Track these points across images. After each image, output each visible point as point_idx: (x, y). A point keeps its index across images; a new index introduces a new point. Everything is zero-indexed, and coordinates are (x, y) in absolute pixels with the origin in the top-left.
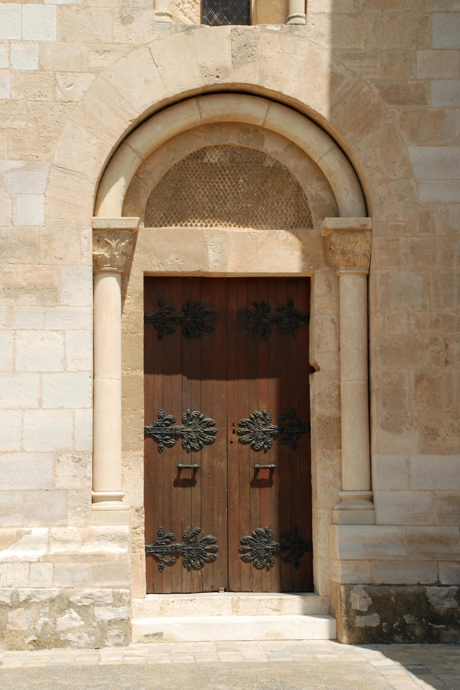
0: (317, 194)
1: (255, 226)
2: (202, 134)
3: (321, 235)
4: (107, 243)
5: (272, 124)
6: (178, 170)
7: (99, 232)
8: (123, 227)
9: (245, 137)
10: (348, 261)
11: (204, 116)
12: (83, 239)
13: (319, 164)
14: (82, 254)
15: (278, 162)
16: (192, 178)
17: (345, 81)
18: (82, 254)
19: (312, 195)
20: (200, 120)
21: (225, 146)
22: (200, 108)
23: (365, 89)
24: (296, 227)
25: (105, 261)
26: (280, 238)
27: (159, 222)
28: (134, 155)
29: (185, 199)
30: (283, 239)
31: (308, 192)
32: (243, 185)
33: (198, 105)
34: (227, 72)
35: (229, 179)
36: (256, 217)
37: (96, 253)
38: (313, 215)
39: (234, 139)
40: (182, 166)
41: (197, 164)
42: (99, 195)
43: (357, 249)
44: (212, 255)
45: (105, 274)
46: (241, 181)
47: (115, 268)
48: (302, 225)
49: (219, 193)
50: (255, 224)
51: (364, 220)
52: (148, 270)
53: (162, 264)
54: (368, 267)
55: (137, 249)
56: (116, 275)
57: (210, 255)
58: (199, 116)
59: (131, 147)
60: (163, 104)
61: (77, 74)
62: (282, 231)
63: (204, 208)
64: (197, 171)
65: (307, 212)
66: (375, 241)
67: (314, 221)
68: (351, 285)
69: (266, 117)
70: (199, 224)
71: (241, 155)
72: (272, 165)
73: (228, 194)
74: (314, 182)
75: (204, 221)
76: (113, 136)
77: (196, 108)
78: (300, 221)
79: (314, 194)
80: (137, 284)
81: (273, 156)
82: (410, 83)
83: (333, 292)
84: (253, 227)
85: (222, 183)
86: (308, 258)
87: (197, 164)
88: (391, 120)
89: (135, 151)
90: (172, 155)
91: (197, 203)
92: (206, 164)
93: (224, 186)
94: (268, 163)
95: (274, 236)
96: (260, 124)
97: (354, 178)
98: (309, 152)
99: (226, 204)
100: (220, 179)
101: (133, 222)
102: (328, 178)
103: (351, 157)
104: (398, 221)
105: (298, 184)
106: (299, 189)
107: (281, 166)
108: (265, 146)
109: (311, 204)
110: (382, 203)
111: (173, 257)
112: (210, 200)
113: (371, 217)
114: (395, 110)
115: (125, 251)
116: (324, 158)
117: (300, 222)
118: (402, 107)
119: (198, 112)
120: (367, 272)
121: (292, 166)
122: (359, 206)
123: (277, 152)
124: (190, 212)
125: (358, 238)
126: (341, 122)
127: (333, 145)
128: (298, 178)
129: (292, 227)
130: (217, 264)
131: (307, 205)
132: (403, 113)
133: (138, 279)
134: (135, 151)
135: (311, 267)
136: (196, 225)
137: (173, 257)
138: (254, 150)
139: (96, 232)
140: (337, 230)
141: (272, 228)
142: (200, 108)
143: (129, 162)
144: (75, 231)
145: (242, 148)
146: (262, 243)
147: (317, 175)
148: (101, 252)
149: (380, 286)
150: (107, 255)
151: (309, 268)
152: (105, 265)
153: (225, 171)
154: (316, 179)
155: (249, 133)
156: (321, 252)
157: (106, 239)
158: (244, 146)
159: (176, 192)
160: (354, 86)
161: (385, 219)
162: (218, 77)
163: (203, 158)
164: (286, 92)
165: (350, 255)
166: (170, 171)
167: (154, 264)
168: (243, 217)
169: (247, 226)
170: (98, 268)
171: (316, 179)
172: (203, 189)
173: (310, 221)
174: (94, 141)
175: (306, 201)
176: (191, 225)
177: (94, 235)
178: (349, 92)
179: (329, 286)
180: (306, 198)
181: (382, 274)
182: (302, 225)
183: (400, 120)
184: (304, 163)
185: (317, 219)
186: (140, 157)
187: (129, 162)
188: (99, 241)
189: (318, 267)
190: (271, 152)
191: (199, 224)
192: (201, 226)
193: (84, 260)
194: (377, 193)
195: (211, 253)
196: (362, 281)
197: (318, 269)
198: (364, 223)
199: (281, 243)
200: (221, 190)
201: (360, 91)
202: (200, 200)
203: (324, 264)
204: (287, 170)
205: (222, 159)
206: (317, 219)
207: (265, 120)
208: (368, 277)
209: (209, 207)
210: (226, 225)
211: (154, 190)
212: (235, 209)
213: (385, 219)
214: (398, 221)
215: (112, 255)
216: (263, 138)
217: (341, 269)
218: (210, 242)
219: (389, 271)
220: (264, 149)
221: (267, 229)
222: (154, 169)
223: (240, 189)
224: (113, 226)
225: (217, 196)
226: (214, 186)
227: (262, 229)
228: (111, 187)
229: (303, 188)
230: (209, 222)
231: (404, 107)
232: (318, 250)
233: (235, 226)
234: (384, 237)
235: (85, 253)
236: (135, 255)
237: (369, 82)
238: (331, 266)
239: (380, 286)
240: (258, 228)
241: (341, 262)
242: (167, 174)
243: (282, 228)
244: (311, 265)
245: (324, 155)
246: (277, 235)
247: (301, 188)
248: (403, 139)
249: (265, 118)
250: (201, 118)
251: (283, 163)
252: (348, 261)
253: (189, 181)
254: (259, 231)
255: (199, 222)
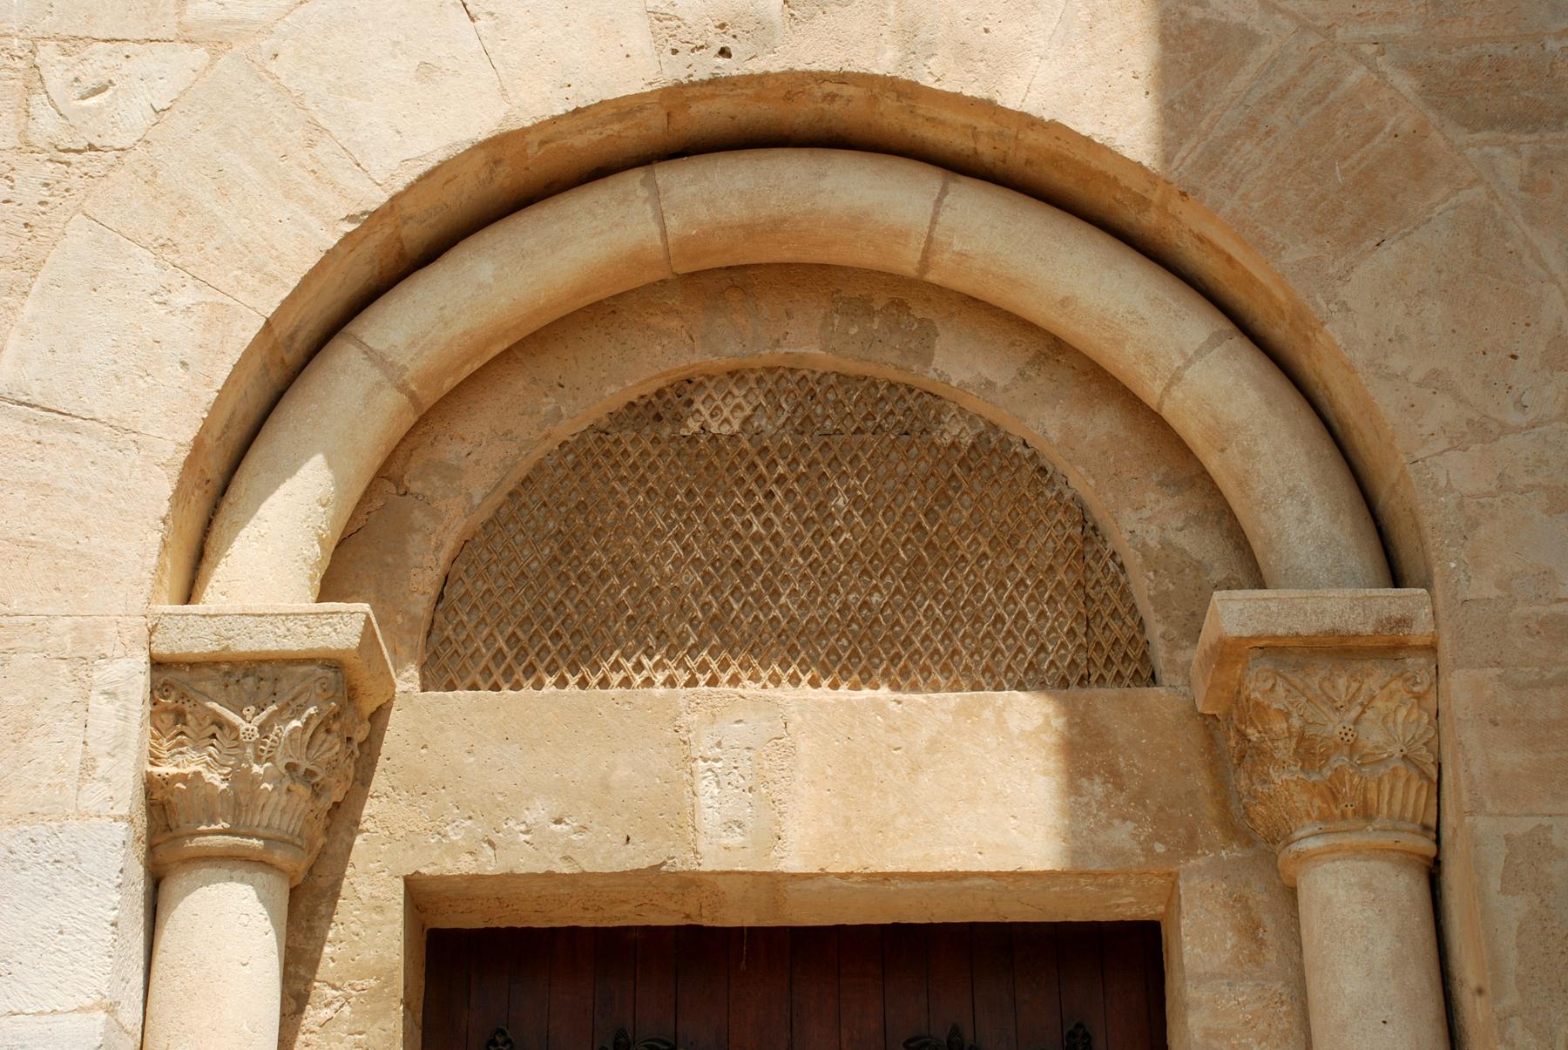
0: (1165, 544)
1: (902, 679)
2: (675, 323)
3: (1194, 707)
4: (220, 723)
5: (960, 254)
6: (576, 465)
7: (184, 675)
8: (293, 645)
9: (853, 331)
10: (1334, 795)
11: (673, 223)
12: (97, 701)
13: (1166, 413)
14: (87, 767)
15: (995, 428)
16: (633, 492)
17: (1265, 50)
18: (87, 767)
19: (1144, 545)
20: (659, 243)
21: (770, 370)
22: (656, 195)
23: (1355, 75)
24: (1083, 681)
25: (209, 807)
26: (1014, 723)
27: (487, 673)
28: (376, 374)
29: (603, 577)
30: (1028, 728)
31: (1126, 536)
32: (848, 516)
33: (649, 183)
34: (761, 28)
35: (789, 493)
36: (907, 642)
37: (166, 769)
38: (1156, 629)
39: (806, 339)
40: (592, 450)
41: (655, 441)
42: (213, 540)
43: (1372, 736)
44: (713, 802)
45: (205, 871)
46: (841, 501)
47: (255, 841)
48: (1109, 676)
49: (746, 551)
50: (905, 673)
51: (1390, 601)
52: (423, 871)
53: (491, 844)
54: (1432, 822)
55: (379, 782)
56: (261, 877)
57: (704, 800)
58: (654, 228)
59: (361, 344)
60: (505, 179)
61: (128, 48)
62: (1021, 696)
63: (683, 609)
64: (653, 467)
65: (1129, 620)
66: (1460, 688)
67: (1160, 655)
68: (1353, 911)
69: (934, 222)
70: (660, 677)
71: (838, 403)
72: (967, 440)
73: (786, 555)
74: (1153, 496)
75: (681, 664)
76: (271, 279)
77: (643, 193)
78: (1095, 648)
79: (1153, 544)
80: (369, 936)
81: (973, 404)
82: (1552, 45)
83: (1271, 956)
84: (895, 687)
85: (758, 510)
86: (1145, 806)
87: (655, 441)
88: (1480, 189)
89: (378, 359)
90: (548, 404)
91: (653, 592)
92: (692, 440)
93: (768, 523)
94: (953, 430)
95: (988, 714)
96: (907, 261)
97: (1326, 449)
98: (1124, 361)
99: (776, 594)
100: (749, 494)
101: (343, 627)
102: (1213, 463)
103: (1306, 364)
104: (1559, 600)
105: (1083, 510)
106: (1090, 530)
107: (1005, 441)
108: (938, 361)
109: (1143, 586)
110: (1474, 525)
111: (538, 812)
112: (706, 576)
113: (1427, 584)
114: (1497, 151)
115: (305, 764)
116: (1188, 374)
117: (1100, 662)
118: (1526, 138)
119: (648, 207)
120: (1425, 845)
121: (1054, 435)
122: (1360, 557)
123: (990, 384)
124: (621, 626)
125: (1372, 684)
126: (1255, 205)
127: (1224, 325)
128: (1082, 482)
129: (1064, 683)
130: (735, 839)
131: (1125, 593)
132: (1534, 161)
133: (380, 909)
134: (378, 359)
135: (1160, 848)
136: (648, 682)
137: (538, 812)
138: (892, 386)
139: (169, 676)
140: (1275, 650)
141: (976, 687)
142: (656, 195)
143: (353, 405)
144: (64, 668)
145: (842, 378)
146: (934, 745)
147: (1163, 470)
148: (189, 763)
149: (1503, 891)
150: (215, 778)
151: (1149, 852)
152: (203, 828)
153: (772, 464)
154: (1161, 484)
155: (870, 313)
156: (1200, 781)
157: (214, 705)
158: (851, 367)
159: (566, 548)
160: (1304, 70)
161: (1494, 593)
162: (724, 52)
163: (678, 420)
164: (1012, 98)
165: (1340, 760)
166: (539, 467)
167: (453, 844)
168: (855, 647)
169: (867, 679)
170: (170, 841)
171: (1161, 484)
172: (678, 536)
173: (1145, 658)
174: (182, 299)
175: (1122, 579)
176: (626, 682)
177: (158, 690)
178: (1283, 92)
179: (1251, 930)
180: (1121, 566)
181: (1508, 839)
182: (1109, 676)
183: (1522, 189)
184: (1102, 425)
185: (1173, 645)
186: (402, 388)
187: (353, 405)
188: (180, 716)
189: (1190, 846)
190: (962, 386)
191: (660, 677)
192: (671, 682)
193: (94, 796)
194: (1443, 482)
195: (707, 788)
196: (1406, 887)
197: (1195, 856)
198: (1396, 612)
199: (1021, 745)
200: (757, 538)
201: (1333, 84)
202: (665, 579)
203: (1216, 832)
204: (1034, 456)
205: (760, 422)
206: (1173, 645)
207: (930, 240)
208: (1433, 873)
209: (705, 607)
210: (777, 682)
211: (465, 545)
212: (814, 612)
213: (1494, 593)
214: (1559, 600)
215: (239, 777)
216: (927, 333)
217: (1298, 834)
218: (704, 746)
219: (1546, 821)
220: (932, 374)
221: (955, 687)
222: (473, 457)
223: (835, 534)
224: (246, 645)
225: (737, 563)
226: (727, 523)
227: (936, 689)
228: (262, 499)
229: (1106, 524)
230: (704, 667)
231: (1535, 137)
232: (1188, 771)
233: (814, 683)
234: (1498, 671)
235: (104, 763)
236: (370, 808)
237: (1369, 50)
238: (1250, 843)
239: (1503, 891)
240: (914, 688)
241: (1301, 800)
242: (527, 481)
243: (1020, 686)
244: (1161, 839)
245: (1189, 362)
246: (999, 712)
247: (1094, 528)
248: (1543, 265)
249: (931, 229)
250: (664, 234)
251: (1017, 432)
252: (1334, 795)
253: (621, 505)
254: (918, 698)
255: (659, 666)
